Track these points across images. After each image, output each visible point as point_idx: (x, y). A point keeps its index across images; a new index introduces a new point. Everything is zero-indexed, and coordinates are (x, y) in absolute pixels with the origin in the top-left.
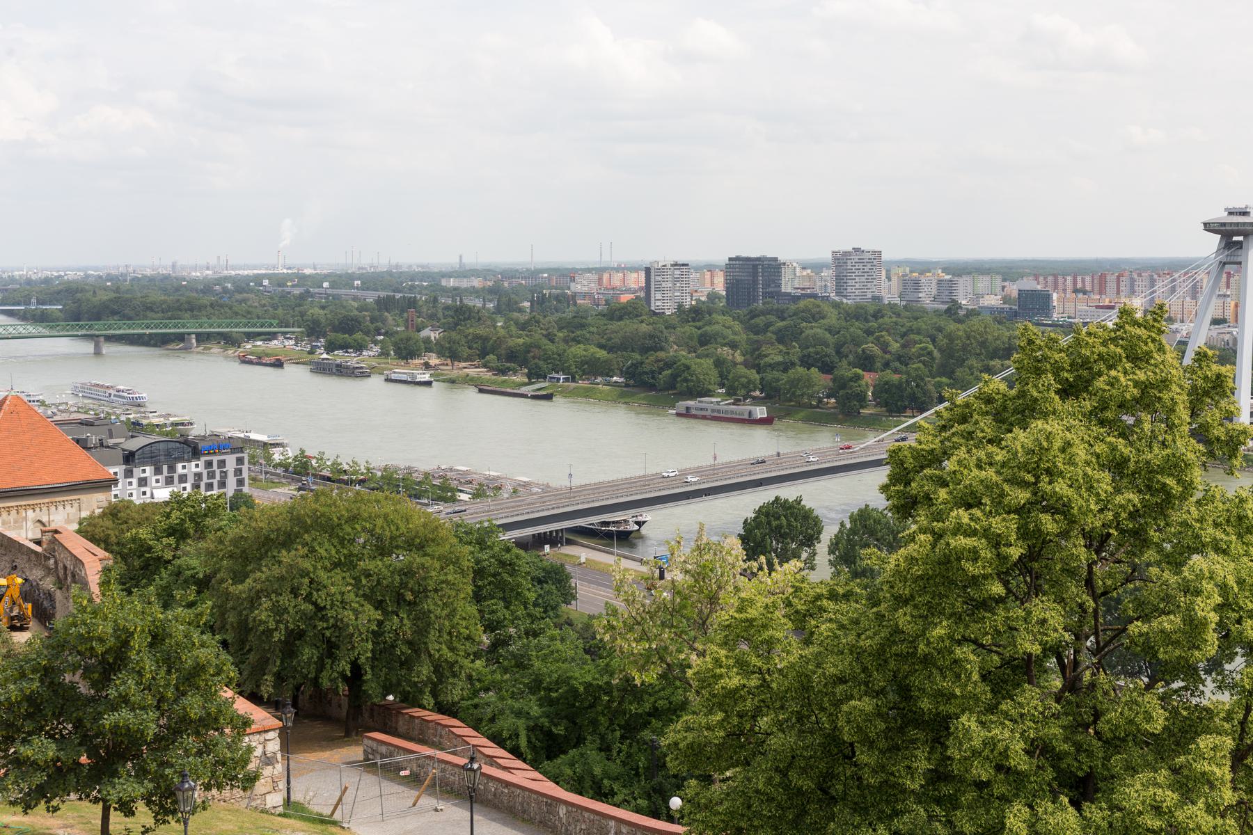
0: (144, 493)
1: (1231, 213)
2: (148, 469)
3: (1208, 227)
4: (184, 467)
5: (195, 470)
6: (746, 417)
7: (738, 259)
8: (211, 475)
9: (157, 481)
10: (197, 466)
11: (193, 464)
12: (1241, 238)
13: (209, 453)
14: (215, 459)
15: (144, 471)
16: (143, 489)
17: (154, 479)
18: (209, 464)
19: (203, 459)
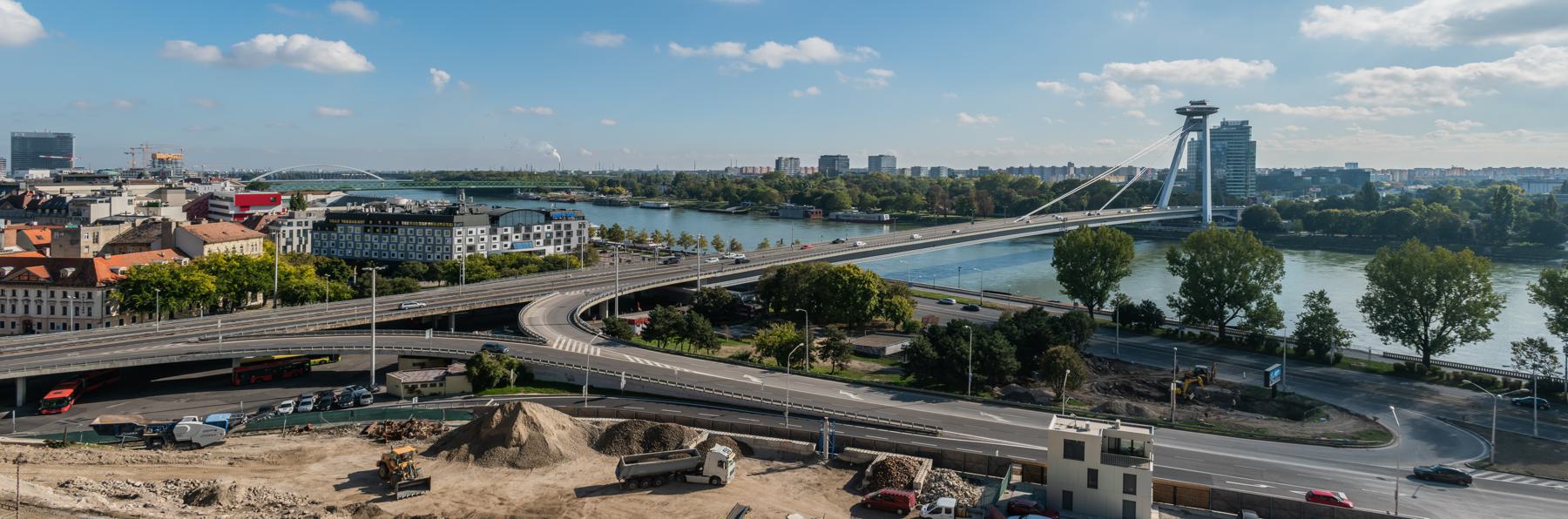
0: (506, 246)
1: (1192, 103)
2: (509, 228)
3: (1181, 111)
4: (538, 228)
5: (546, 230)
8: (559, 234)
10: (549, 228)
11: (546, 226)
12: (1201, 117)
13: (558, 220)
14: (563, 223)
15: (506, 230)
16: (505, 243)
17: (514, 235)
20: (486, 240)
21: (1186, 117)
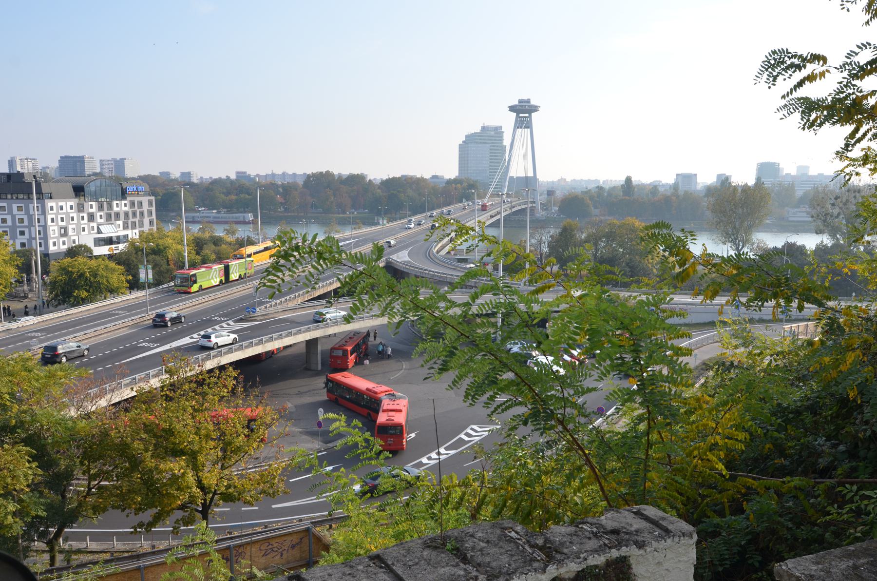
1: (520, 101)
3: (512, 109)
6: (241, 219)
7: (66, 157)
8: (134, 214)
9: (101, 217)
10: (125, 205)
11: (123, 202)
12: (527, 115)
14: (136, 199)
17: (99, 214)
18: (132, 204)
19: (129, 199)
20: (76, 221)
21: (515, 114)
